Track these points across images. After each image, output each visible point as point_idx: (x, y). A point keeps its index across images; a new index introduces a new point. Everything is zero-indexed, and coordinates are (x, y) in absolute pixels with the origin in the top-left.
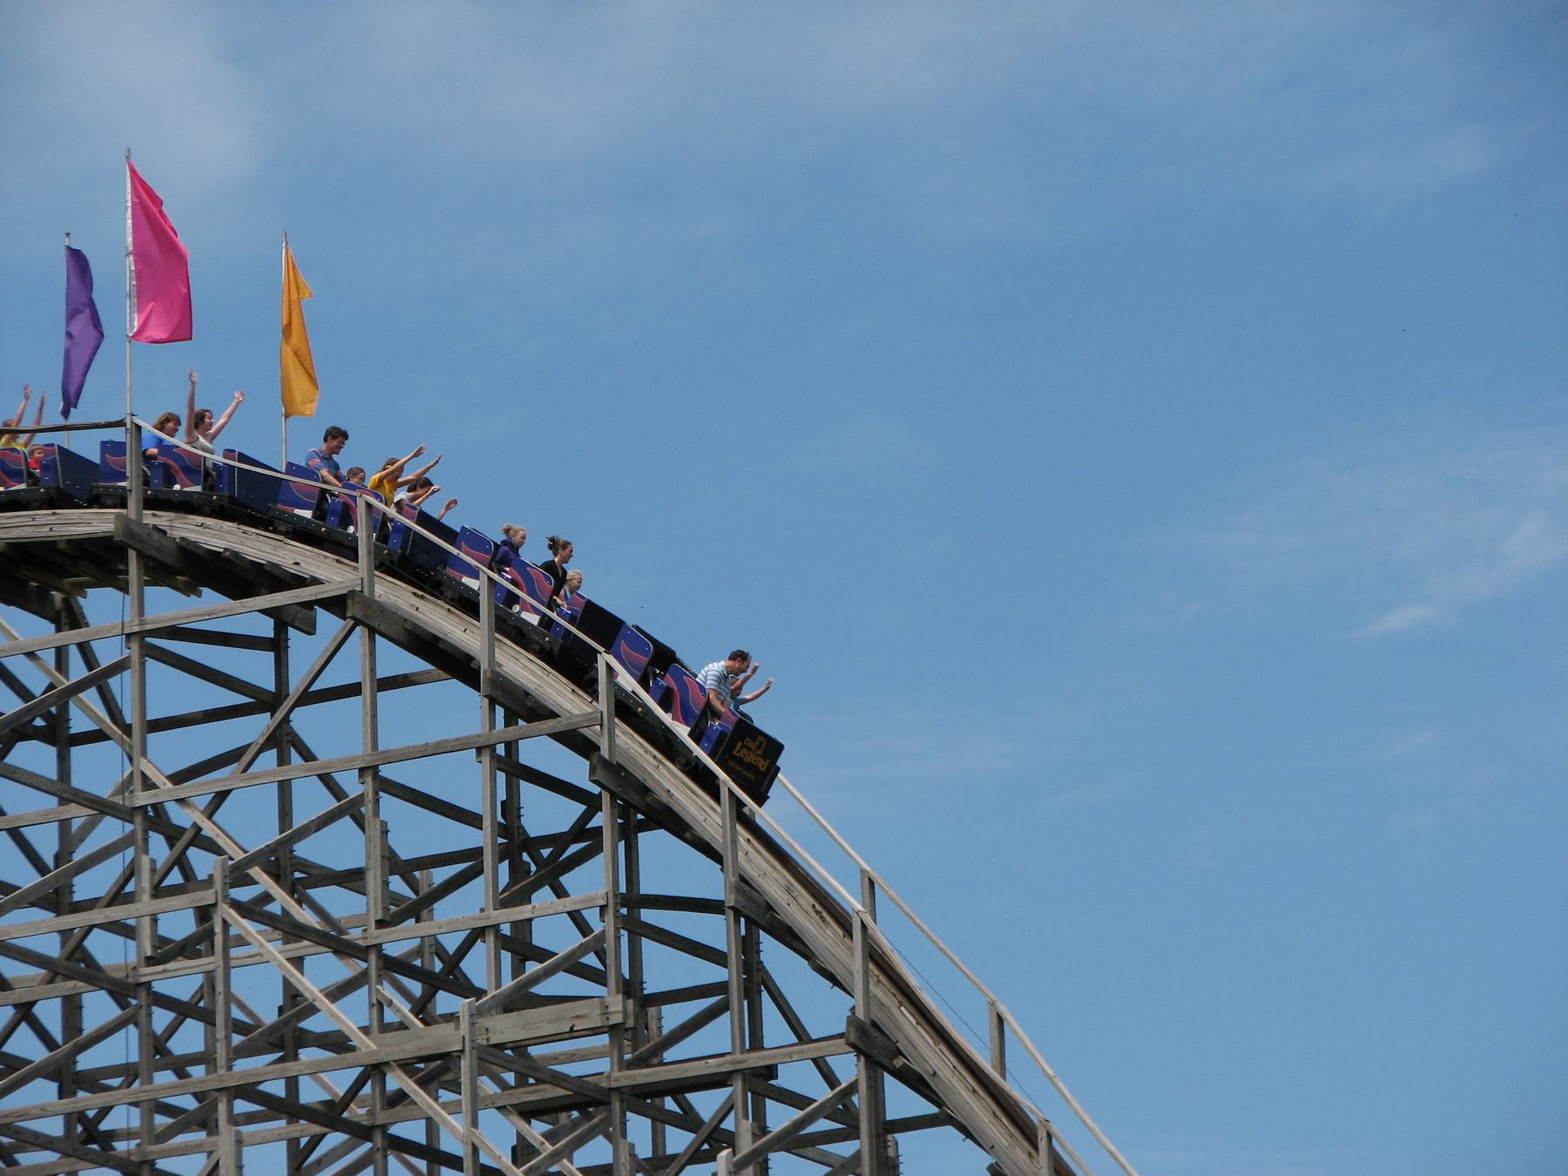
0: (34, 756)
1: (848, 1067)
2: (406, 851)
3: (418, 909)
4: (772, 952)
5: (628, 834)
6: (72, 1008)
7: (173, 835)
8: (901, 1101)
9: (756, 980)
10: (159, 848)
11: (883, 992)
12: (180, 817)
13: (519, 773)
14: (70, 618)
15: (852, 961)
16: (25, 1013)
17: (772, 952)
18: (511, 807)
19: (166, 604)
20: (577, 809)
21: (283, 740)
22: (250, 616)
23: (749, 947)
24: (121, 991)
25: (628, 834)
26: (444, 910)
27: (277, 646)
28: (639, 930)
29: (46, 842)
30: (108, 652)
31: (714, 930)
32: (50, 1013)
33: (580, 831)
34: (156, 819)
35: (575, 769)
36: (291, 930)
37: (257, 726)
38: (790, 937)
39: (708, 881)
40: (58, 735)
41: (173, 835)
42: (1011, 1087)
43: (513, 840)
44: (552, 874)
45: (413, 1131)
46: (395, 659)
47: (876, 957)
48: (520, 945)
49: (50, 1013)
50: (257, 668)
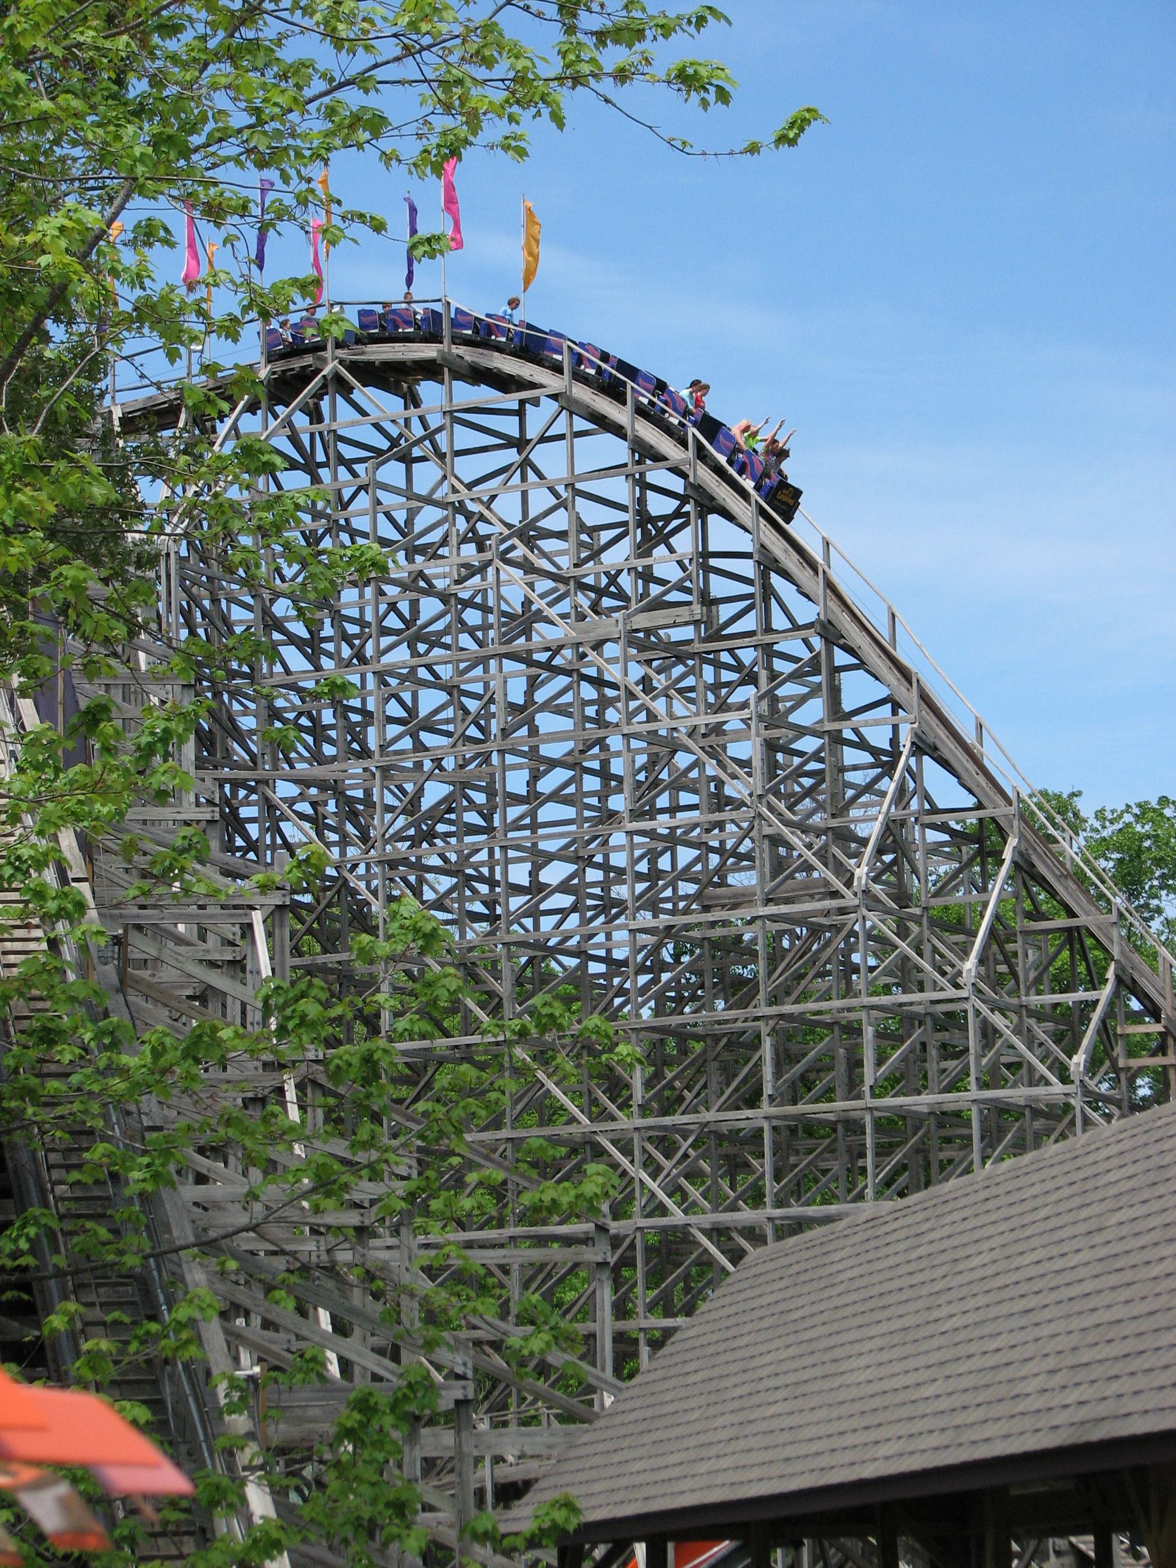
0: (393, 472)
1: (817, 642)
2: (589, 523)
3: (595, 555)
4: (775, 580)
5: (703, 517)
6: (414, 606)
7: (469, 516)
8: (841, 658)
9: (768, 592)
10: (461, 523)
11: (833, 605)
12: (473, 507)
13: (646, 486)
14: (413, 400)
15: (816, 587)
16: (393, 607)
17: (775, 580)
18: (642, 501)
19: (467, 394)
20: (676, 503)
21: (526, 464)
22: (511, 401)
23: (765, 577)
24: (445, 597)
25: (703, 517)
26: (606, 557)
27: (520, 413)
28: (708, 570)
29: (401, 516)
30: (435, 421)
31: (747, 568)
32: (404, 607)
33: (677, 514)
34: (460, 508)
35: (677, 484)
36: (528, 567)
37: (511, 456)
38: (786, 575)
39: (744, 543)
40: (408, 460)
41: (469, 516)
42: (901, 655)
43: (644, 518)
44: (664, 539)
45: (592, 672)
46: (581, 424)
47: (830, 586)
48: (647, 576)
49: (404, 607)
50: (509, 426)
